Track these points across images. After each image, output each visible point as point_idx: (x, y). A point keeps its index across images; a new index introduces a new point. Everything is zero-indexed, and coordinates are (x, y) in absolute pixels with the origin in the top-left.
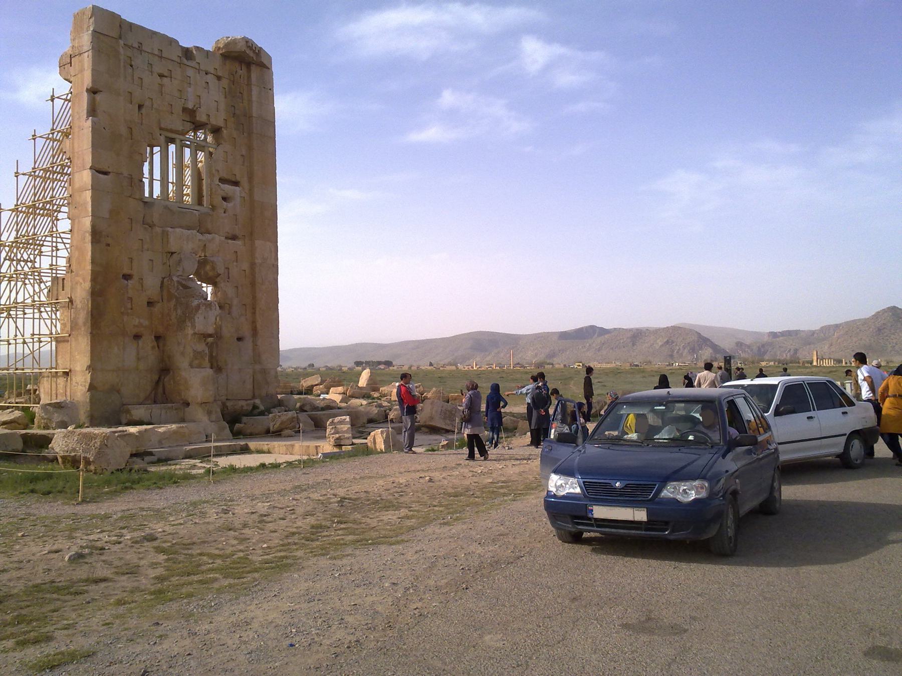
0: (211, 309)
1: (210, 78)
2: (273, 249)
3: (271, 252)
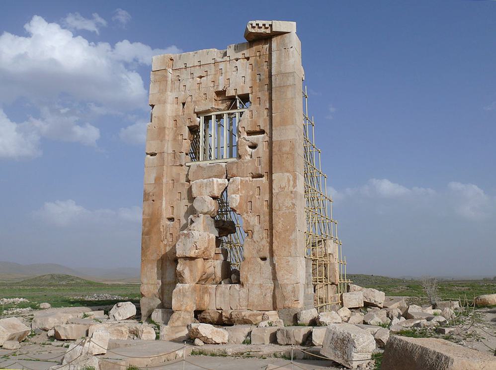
0: (189, 237)
1: (238, 63)
2: (291, 178)
3: (289, 181)
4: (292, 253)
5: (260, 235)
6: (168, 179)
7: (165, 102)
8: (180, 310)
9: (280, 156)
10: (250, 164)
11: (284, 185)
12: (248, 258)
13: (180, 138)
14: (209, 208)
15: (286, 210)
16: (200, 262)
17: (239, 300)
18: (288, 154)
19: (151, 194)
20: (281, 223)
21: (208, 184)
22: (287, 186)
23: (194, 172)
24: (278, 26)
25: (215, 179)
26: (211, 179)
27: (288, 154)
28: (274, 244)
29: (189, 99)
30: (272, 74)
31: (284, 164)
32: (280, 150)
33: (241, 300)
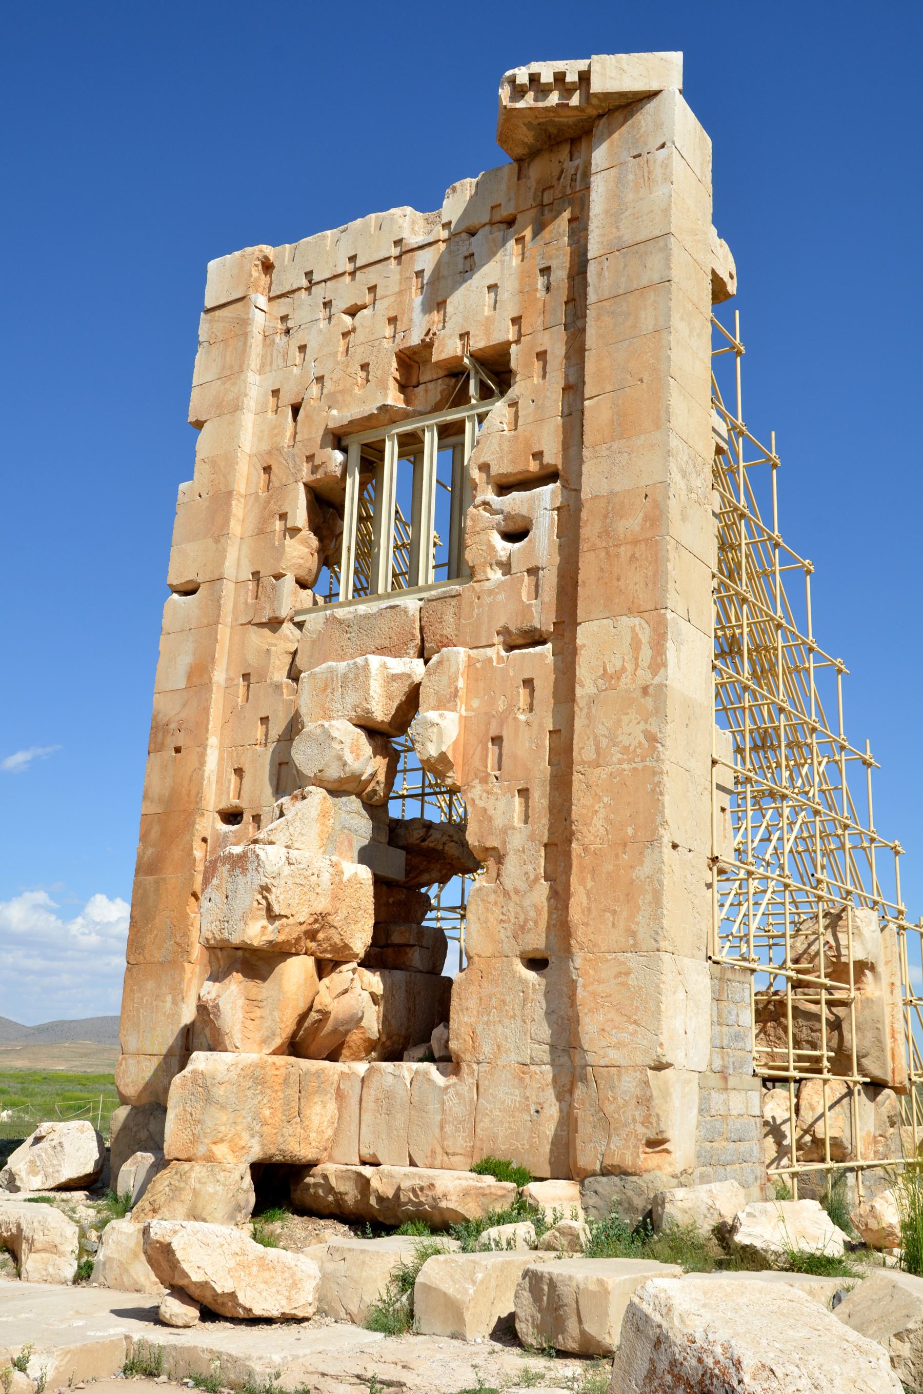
0: (244, 870)
2: (645, 636)
4: (640, 936)
5: (524, 862)
6: (232, 674)
7: (236, 408)
8: (189, 1160)
9: (607, 553)
10: (501, 597)
11: (618, 666)
12: (479, 956)
13: (278, 525)
14: (345, 764)
15: (620, 762)
16: (297, 971)
17: (442, 1128)
18: (635, 542)
19: (173, 726)
20: (602, 813)
21: (351, 676)
22: (630, 667)
23: (313, 642)
24: (614, 73)
25: (375, 661)
26: (360, 660)
27: (635, 542)
28: (572, 901)
29: (315, 389)
30: (590, 255)
31: (622, 583)
32: (606, 533)
33: (448, 1129)
